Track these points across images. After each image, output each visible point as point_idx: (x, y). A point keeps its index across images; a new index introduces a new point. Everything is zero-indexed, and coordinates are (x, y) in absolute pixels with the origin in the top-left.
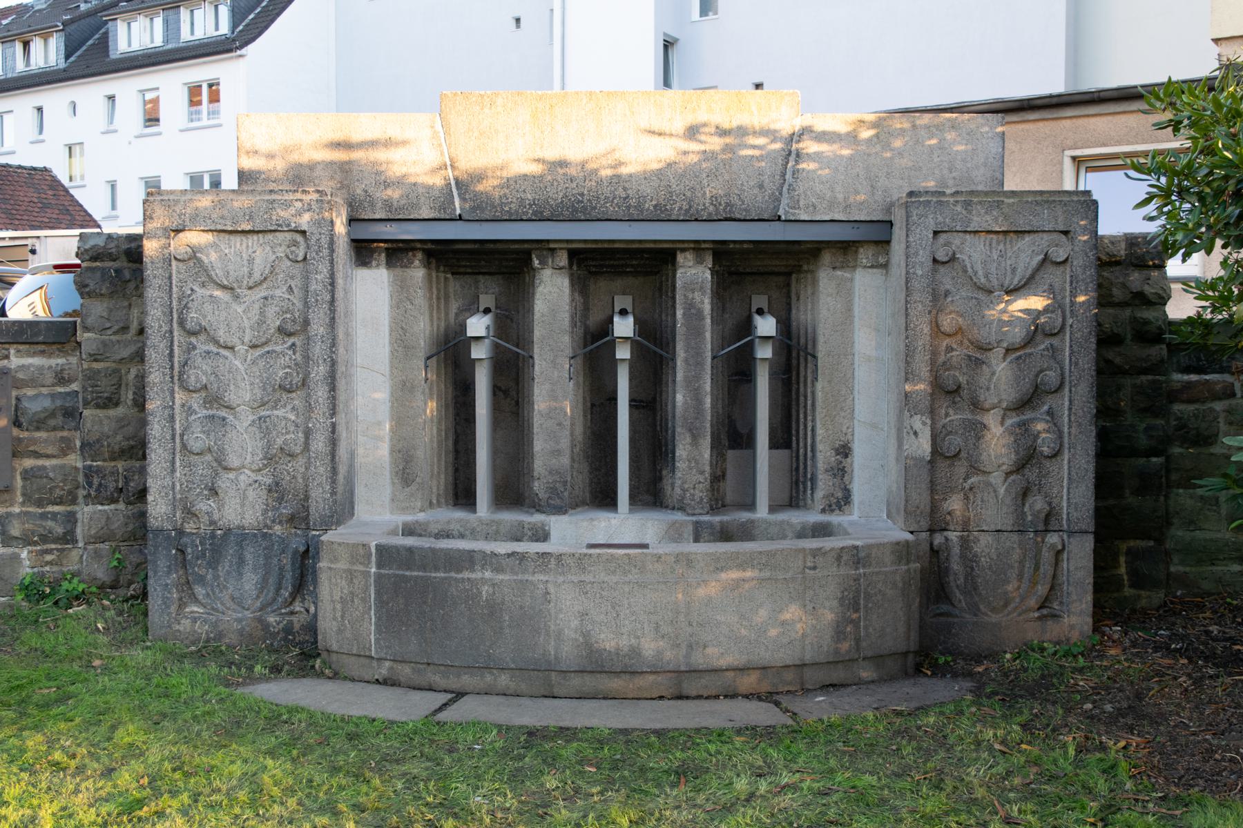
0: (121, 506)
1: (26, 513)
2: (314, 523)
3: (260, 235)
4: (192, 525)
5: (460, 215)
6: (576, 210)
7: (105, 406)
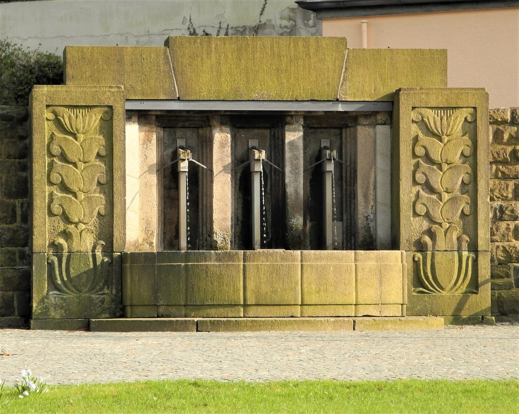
5: (179, 98)
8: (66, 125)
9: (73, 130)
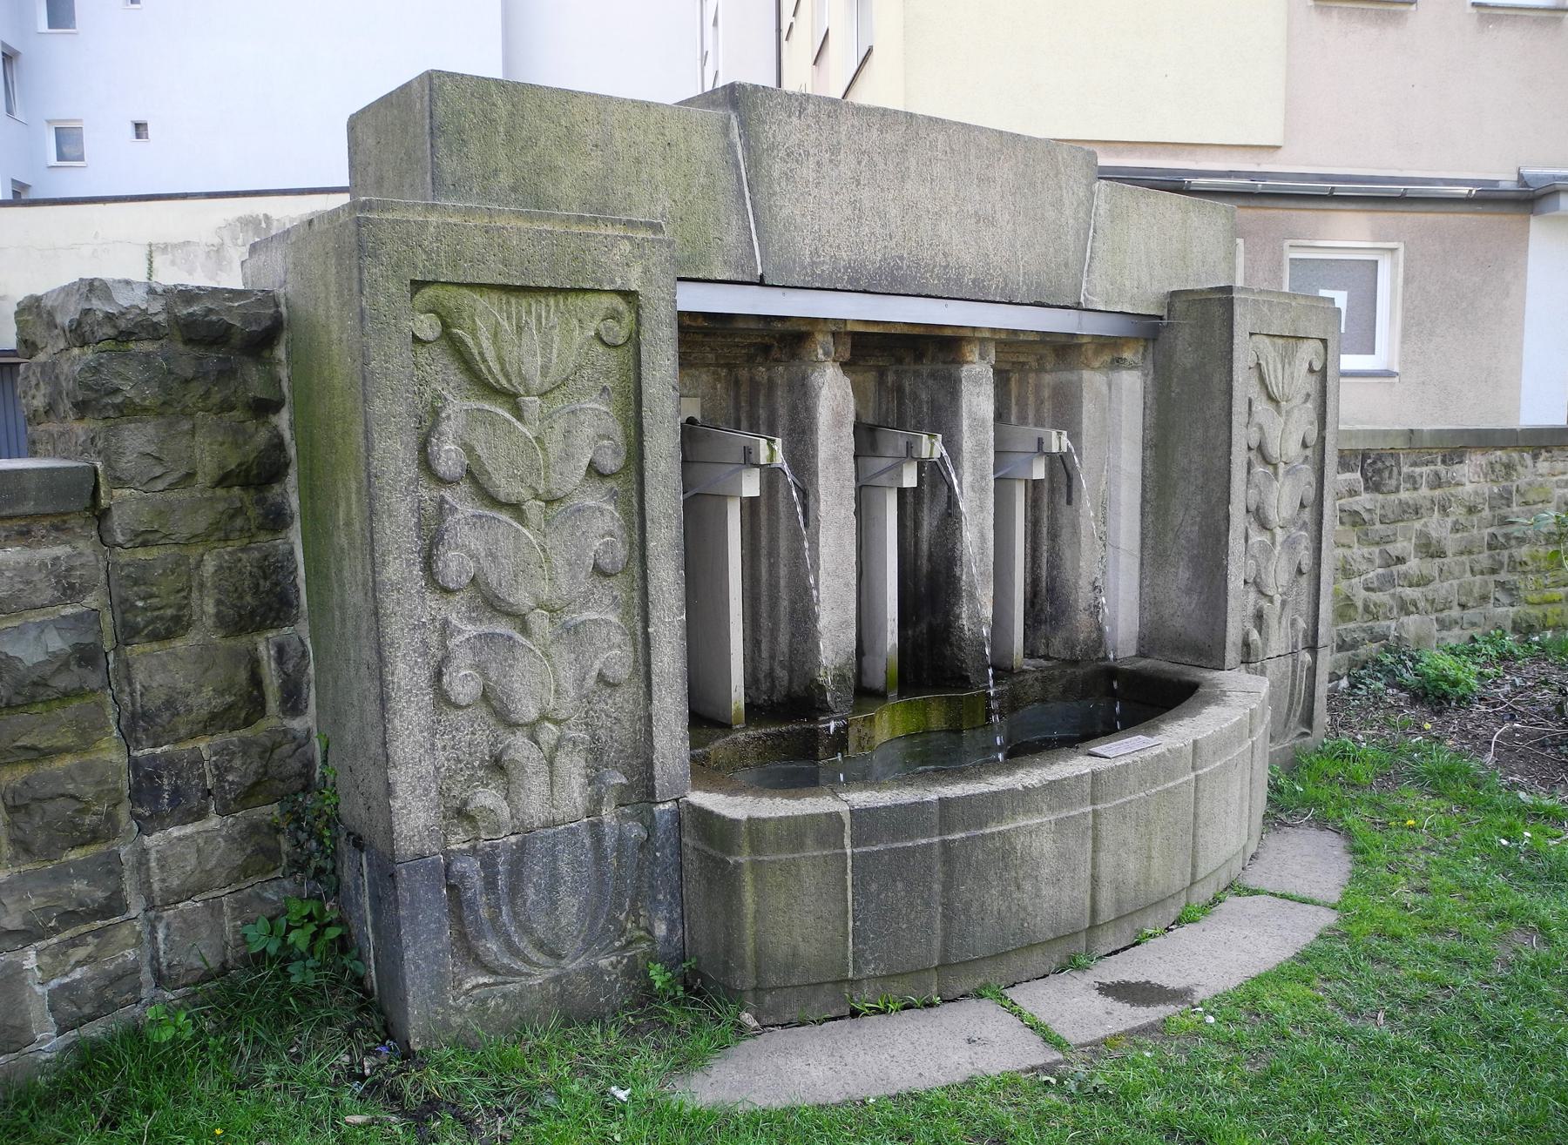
0: (214, 822)
1: (23, 876)
2: (662, 793)
3: (561, 298)
4: (462, 836)
5: (762, 276)
6: (894, 279)
7: (168, 635)
8: (484, 360)
9: (509, 381)
